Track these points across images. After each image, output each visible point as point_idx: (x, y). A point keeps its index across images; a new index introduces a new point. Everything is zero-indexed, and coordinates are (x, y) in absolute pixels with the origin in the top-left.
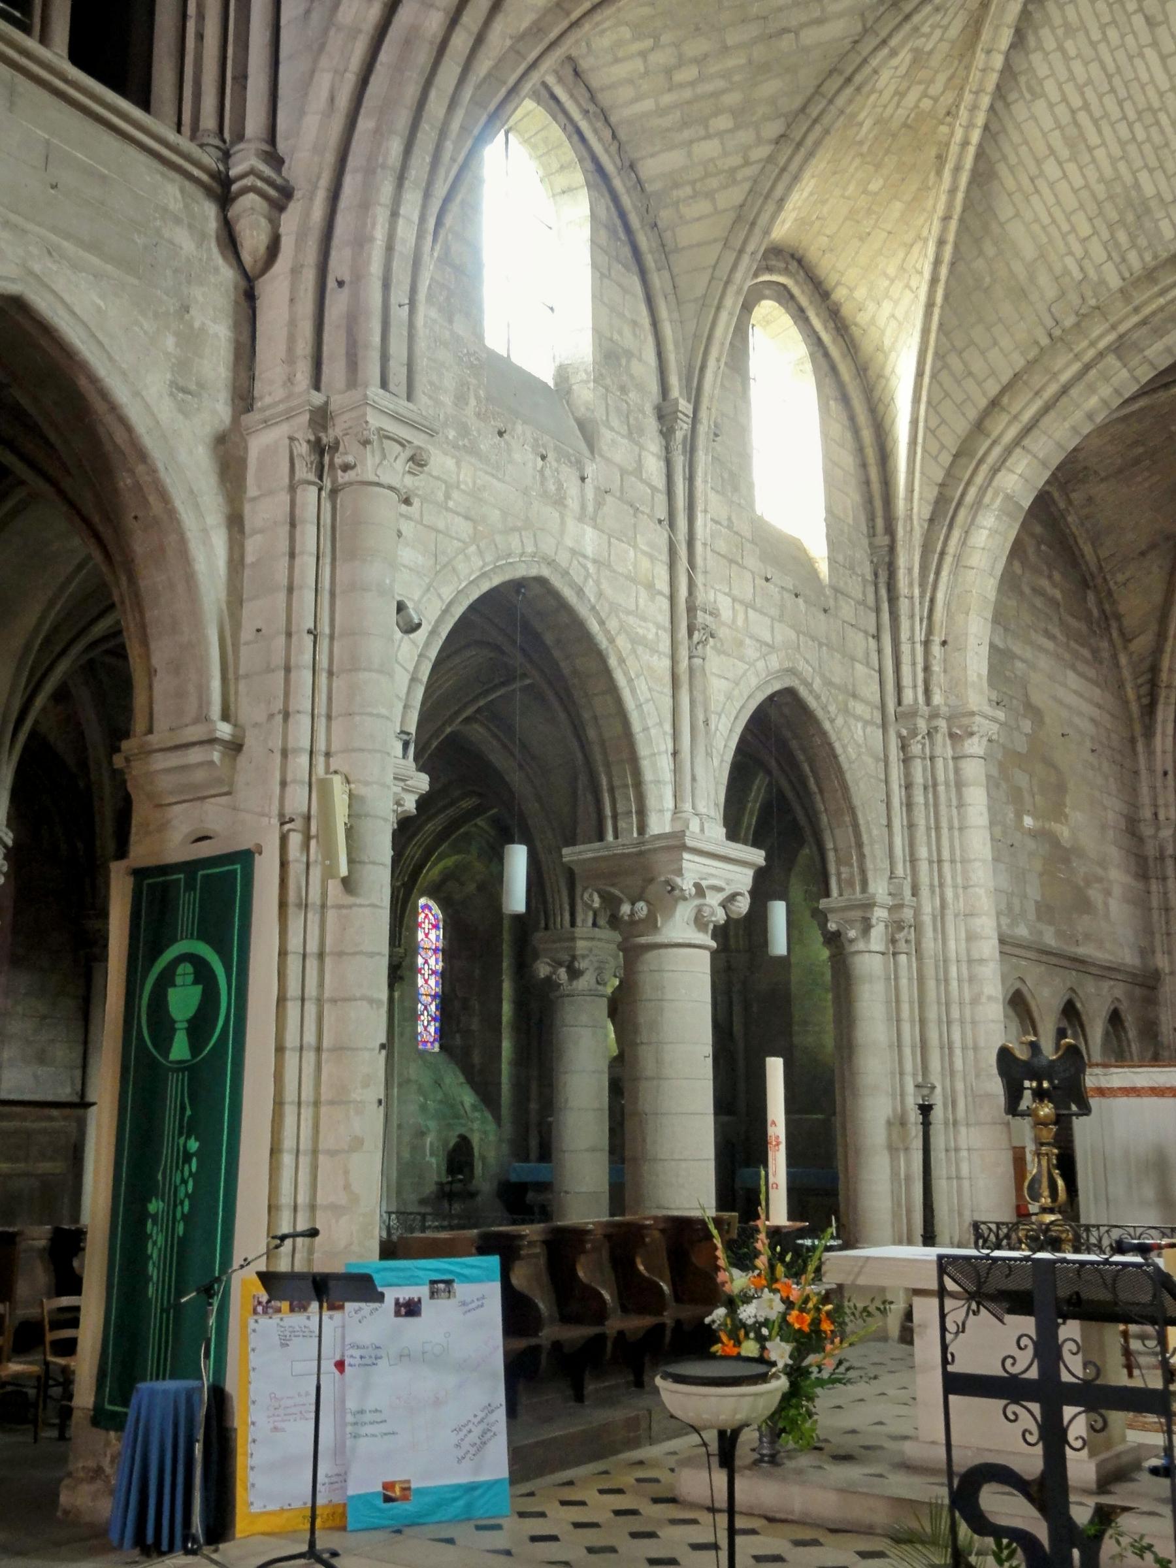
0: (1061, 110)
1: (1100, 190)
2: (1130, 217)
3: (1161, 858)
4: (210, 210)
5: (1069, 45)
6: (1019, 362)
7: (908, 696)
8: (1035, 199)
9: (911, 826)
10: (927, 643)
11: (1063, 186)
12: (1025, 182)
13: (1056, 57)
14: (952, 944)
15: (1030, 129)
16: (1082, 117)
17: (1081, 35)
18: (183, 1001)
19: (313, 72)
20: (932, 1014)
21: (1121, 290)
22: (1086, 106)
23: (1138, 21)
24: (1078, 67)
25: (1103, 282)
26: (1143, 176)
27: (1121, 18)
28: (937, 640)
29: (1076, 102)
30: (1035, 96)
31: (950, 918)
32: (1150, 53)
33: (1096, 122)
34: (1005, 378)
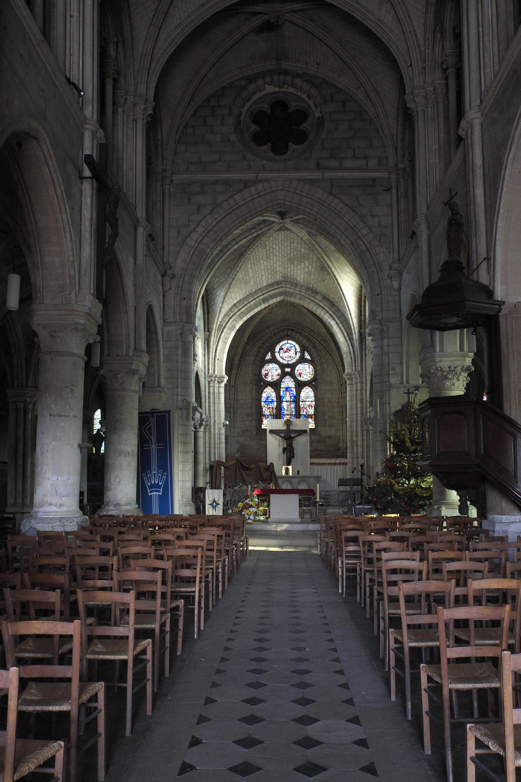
0: (268, 253)
1: (269, 267)
2: (272, 273)
4: (160, 278)
5: (274, 242)
6: (242, 297)
7: (210, 372)
8: (256, 266)
10: (214, 359)
11: (262, 265)
12: (255, 262)
13: (271, 243)
14: (216, 430)
15: (261, 253)
16: (271, 254)
17: (277, 241)
19: (179, 251)
20: (212, 445)
21: (266, 286)
22: (273, 252)
23: (289, 241)
25: (263, 284)
26: (278, 267)
27: (286, 240)
28: (217, 358)
30: (264, 248)
31: (216, 424)
32: (289, 248)
33: (273, 255)
34: (238, 300)
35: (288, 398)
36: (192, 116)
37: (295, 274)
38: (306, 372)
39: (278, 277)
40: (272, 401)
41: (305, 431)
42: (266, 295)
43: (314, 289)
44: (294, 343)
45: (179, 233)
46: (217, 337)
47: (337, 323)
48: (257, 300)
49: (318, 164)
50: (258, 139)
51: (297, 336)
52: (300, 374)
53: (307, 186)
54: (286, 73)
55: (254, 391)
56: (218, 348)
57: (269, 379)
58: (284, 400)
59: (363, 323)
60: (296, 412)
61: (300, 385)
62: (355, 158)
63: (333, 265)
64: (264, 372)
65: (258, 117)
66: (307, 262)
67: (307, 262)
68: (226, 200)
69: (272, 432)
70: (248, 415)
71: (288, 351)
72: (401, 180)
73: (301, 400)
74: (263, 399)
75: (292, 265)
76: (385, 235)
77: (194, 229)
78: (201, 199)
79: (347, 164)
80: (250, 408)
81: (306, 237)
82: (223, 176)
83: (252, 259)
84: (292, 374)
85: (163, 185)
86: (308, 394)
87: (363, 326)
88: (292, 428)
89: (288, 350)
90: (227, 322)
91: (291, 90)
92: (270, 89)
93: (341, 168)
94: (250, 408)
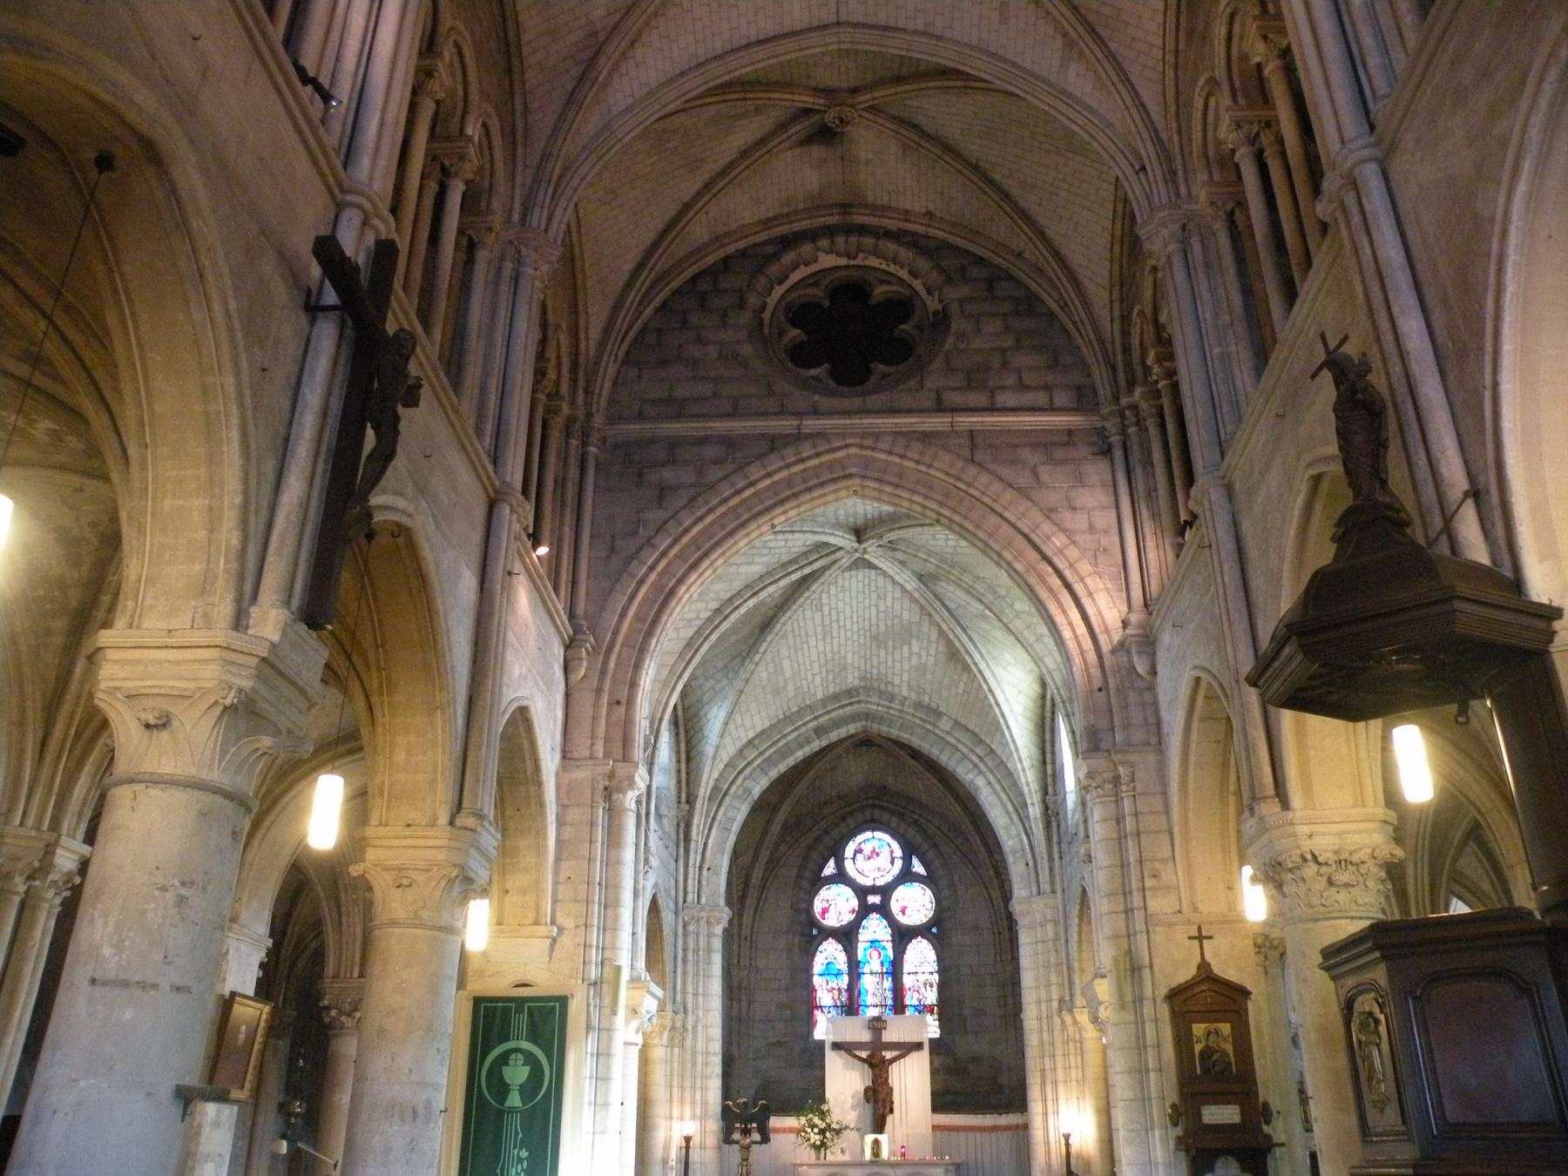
0: (827, 620)
1: (829, 655)
3: (739, 988)
6: (767, 724)
9: (685, 973)
10: (701, 867)
11: (814, 651)
18: (517, 1074)
23: (874, 595)
24: (841, 604)
26: (850, 655)
29: (834, 617)
32: (874, 609)
35: (876, 967)
36: (657, 310)
37: (890, 672)
38: (915, 904)
39: (850, 679)
40: (839, 974)
41: (918, 1046)
42: (821, 720)
43: (934, 705)
44: (887, 838)
45: (612, 549)
46: (707, 816)
47: (989, 783)
48: (803, 730)
49: (939, 399)
50: (801, 356)
51: (895, 821)
52: (903, 911)
53: (917, 446)
54: (862, 230)
55: (796, 950)
56: (710, 842)
57: (831, 921)
58: (866, 969)
59: (1049, 780)
60: (895, 998)
61: (902, 936)
62: (1023, 387)
63: (976, 647)
64: (818, 906)
65: (800, 313)
66: (914, 642)
67: (914, 642)
68: (726, 477)
69: (837, 1046)
70: (781, 1006)
71: (874, 855)
72: (1132, 430)
73: (906, 970)
74: (818, 966)
75: (882, 652)
76: (1105, 550)
77: (649, 540)
78: (668, 474)
79: (1004, 399)
80: (787, 990)
81: (912, 584)
82: (721, 426)
83: (790, 636)
84: (884, 910)
85: (585, 444)
86: (921, 957)
87: (1050, 789)
88: (887, 1037)
89: (875, 853)
90: (732, 783)
91: (873, 262)
92: (827, 261)
93: (992, 409)
94: (787, 990)
